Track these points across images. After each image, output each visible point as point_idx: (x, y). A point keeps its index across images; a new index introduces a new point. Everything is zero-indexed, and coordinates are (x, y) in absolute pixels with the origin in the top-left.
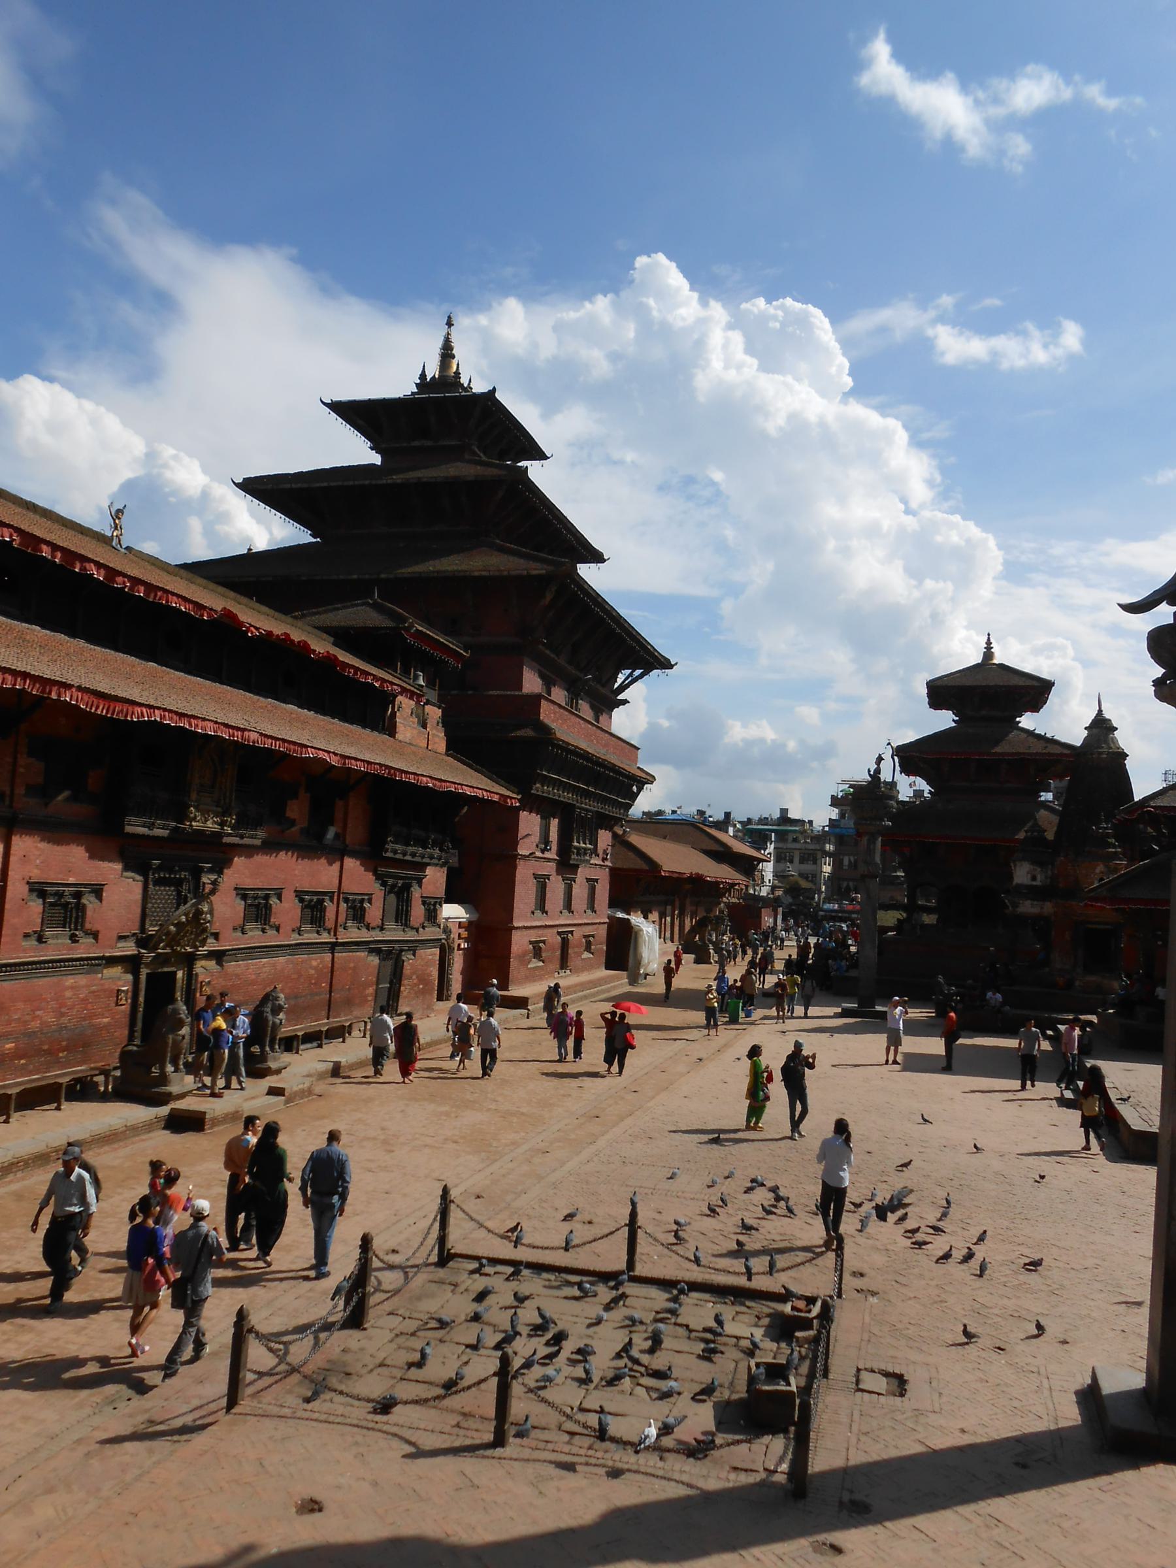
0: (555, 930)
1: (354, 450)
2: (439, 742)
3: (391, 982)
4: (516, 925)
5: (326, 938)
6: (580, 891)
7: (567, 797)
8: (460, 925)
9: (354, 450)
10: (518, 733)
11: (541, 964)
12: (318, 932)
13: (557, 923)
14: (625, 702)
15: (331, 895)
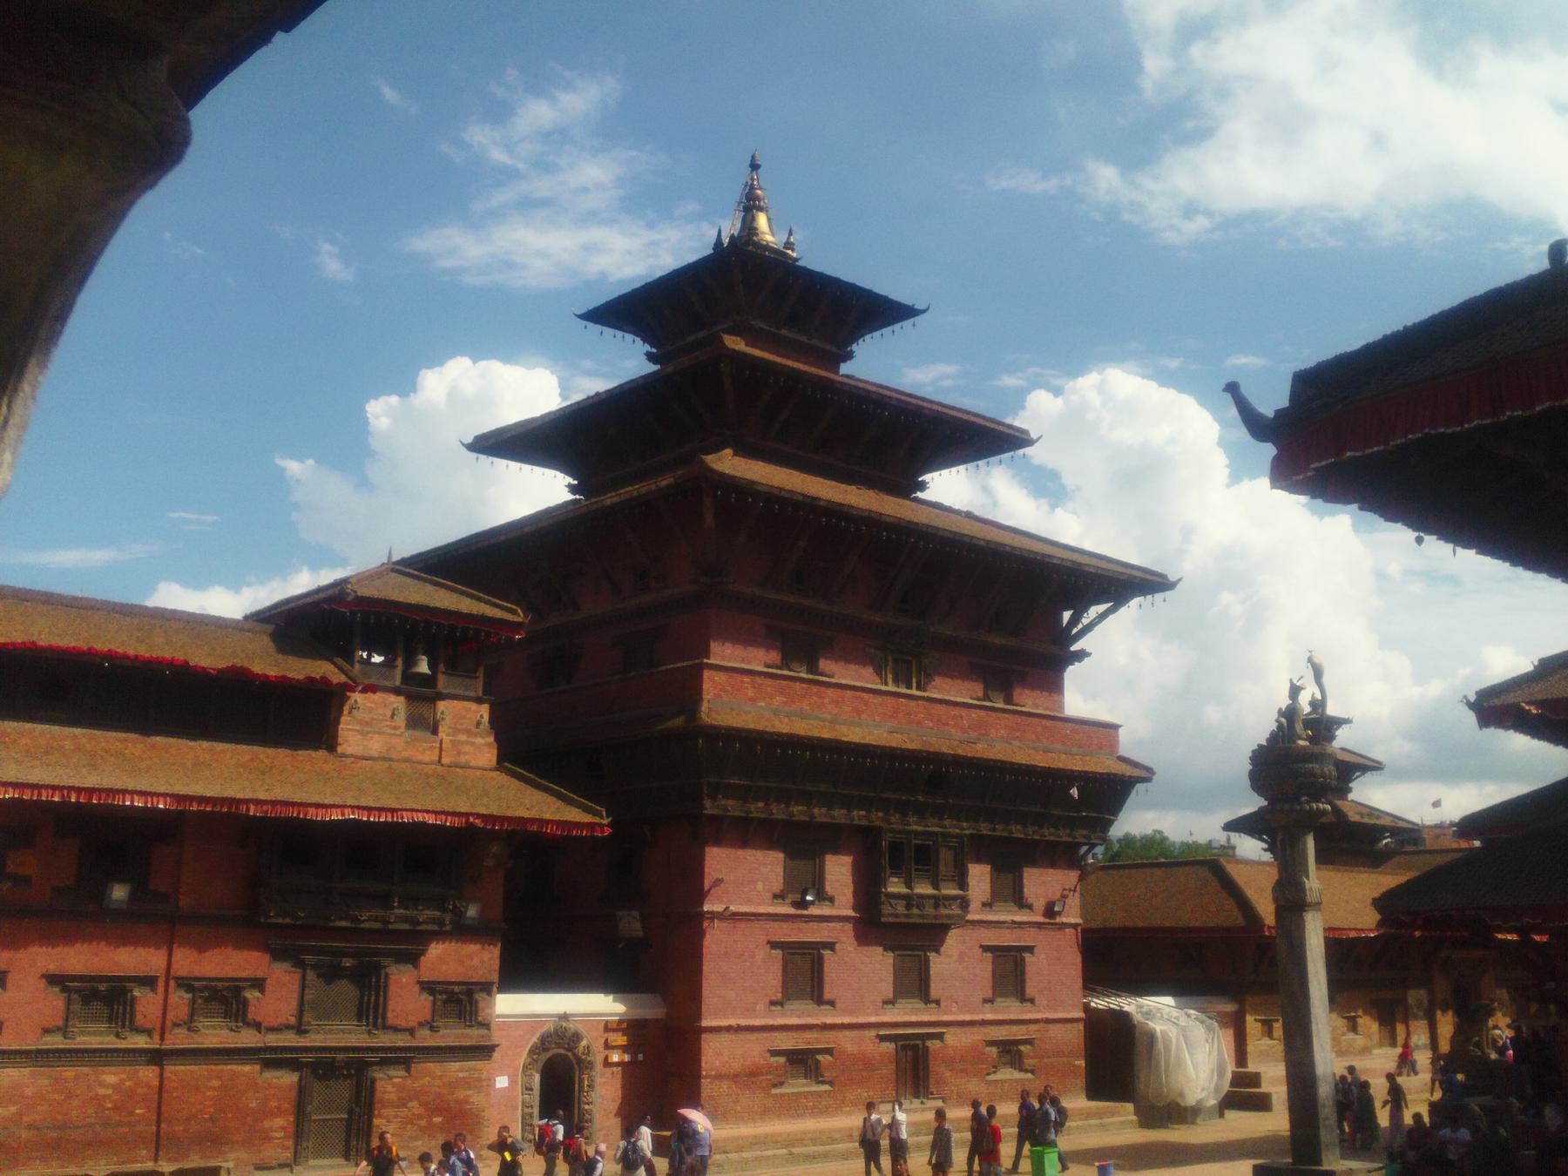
0: (873, 1033)
1: (626, 360)
2: (482, 751)
3: (350, 1112)
4: (705, 1023)
5: (140, 1042)
6: (957, 963)
7: (859, 816)
8: (607, 1028)
9: (626, 360)
10: (669, 724)
11: (826, 1087)
12: (117, 1035)
13: (873, 1019)
14: (1081, 655)
15: (148, 982)
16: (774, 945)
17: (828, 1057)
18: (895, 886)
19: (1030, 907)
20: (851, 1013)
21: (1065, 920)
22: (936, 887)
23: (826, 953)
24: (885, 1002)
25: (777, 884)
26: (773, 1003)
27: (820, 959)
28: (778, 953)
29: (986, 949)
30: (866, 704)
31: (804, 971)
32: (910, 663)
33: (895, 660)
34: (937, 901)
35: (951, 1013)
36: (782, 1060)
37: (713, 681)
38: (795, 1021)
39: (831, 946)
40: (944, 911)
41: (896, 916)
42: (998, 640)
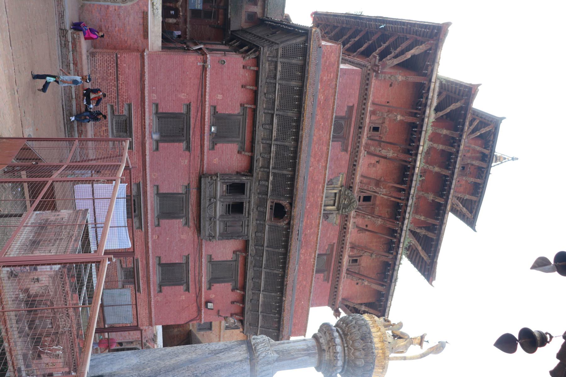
16: (188, 106)
18: (220, 188)
19: (210, 288)
20: (151, 163)
21: (203, 311)
22: (221, 216)
23: (183, 145)
24: (157, 186)
25: (221, 110)
26: (157, 105)
27: (180, 141)
28: (184, 110)
30: (319, 161)
31: (174, 128)
32: (334, 205)
33: (336, 193)
34: (212, 219)
35: (152, 235)
36: (125, 113)
37: (332, 52)
38: (147, 122)
39: (188, 148)
40: (207, 224)
41: (205, 188)
42: (346, 260)
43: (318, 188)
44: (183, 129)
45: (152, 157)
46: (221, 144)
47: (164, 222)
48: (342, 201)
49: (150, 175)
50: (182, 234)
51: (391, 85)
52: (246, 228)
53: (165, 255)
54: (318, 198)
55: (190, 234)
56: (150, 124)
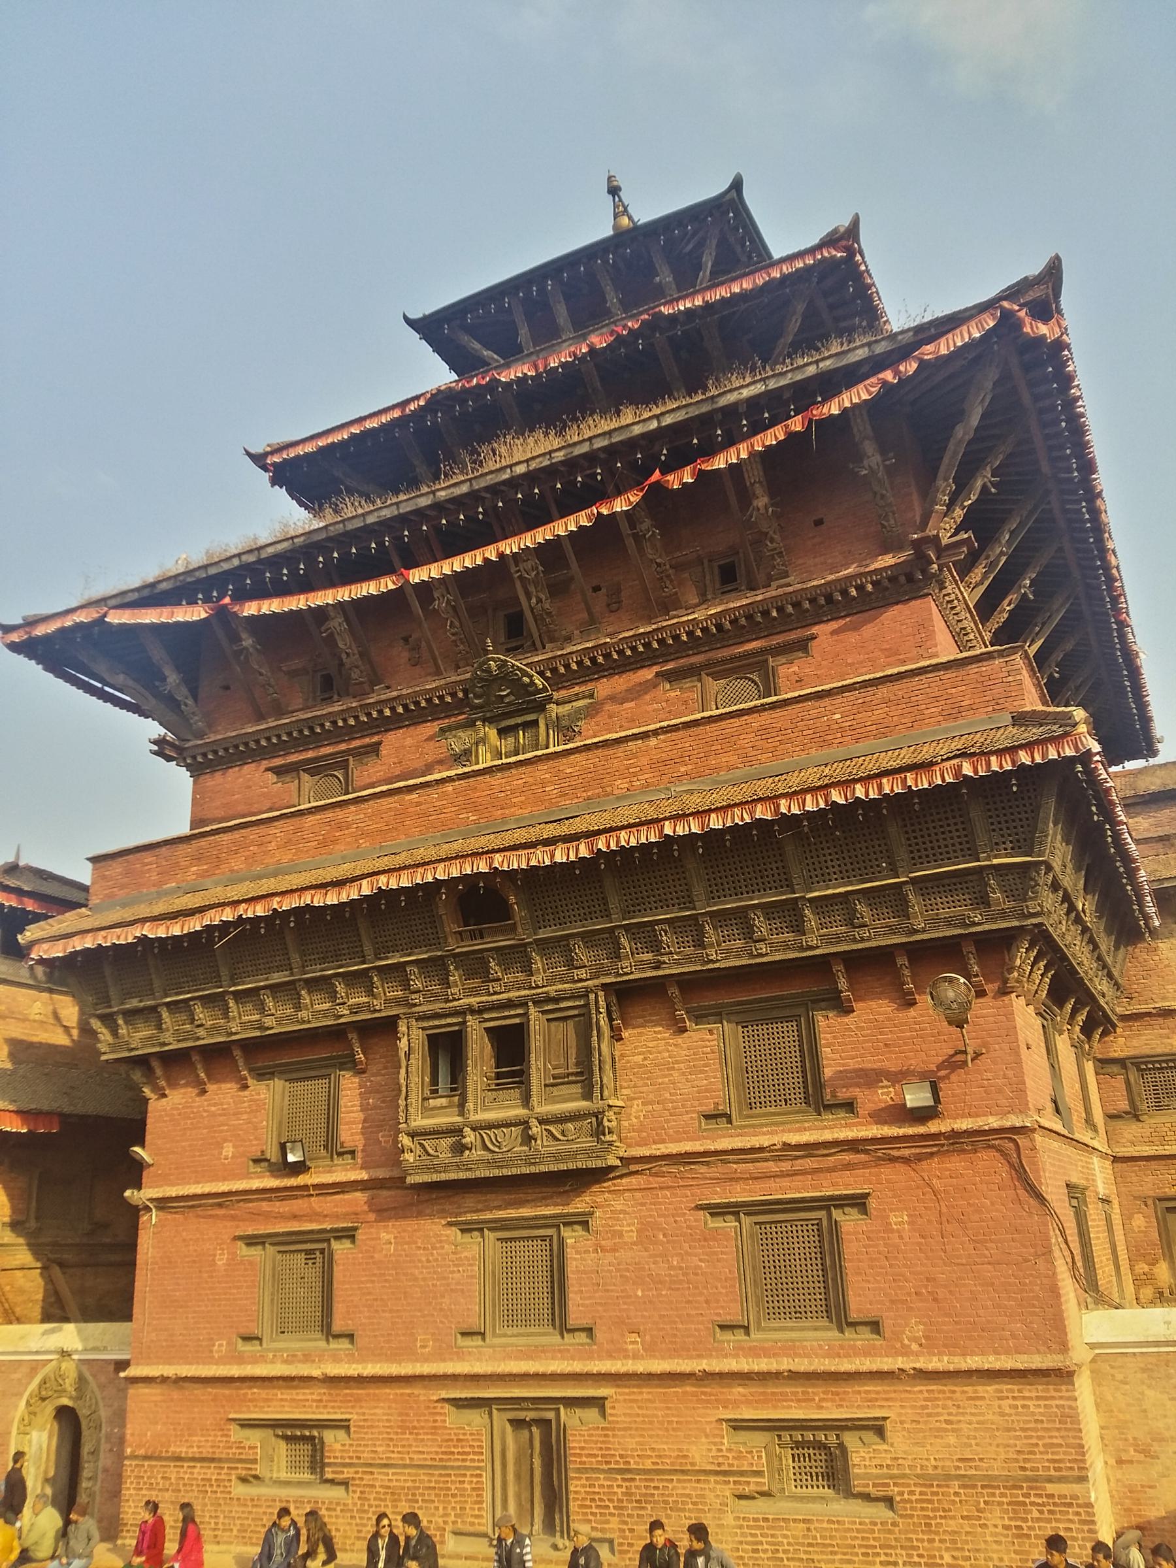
17: (341, 1434)
21: (963, 1125)
23: (340, 1247)
29: (717, 1211)
43: (419, 804)
44: (308, 1252)
45: (378, 1355)
46: (341, 1127)
47: (578, 1309)
48: (510, 704)
49: (426, 1359)
50: (621, 1235)
51: (227, 688)
52: (562, 1005)
53: (707, 1302)
54: (443, 796)
55: (618, 1204)
56: (286, 1362)
